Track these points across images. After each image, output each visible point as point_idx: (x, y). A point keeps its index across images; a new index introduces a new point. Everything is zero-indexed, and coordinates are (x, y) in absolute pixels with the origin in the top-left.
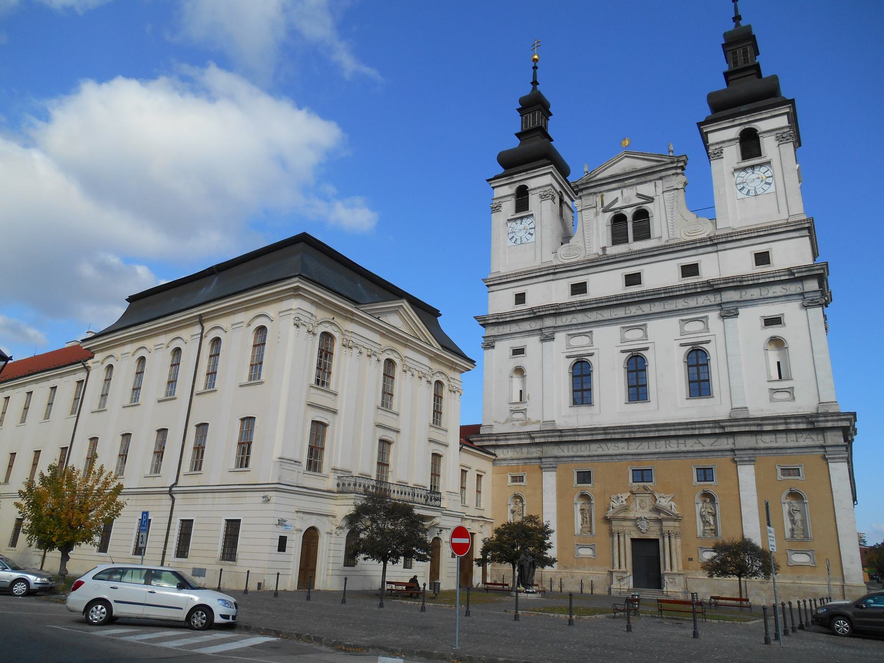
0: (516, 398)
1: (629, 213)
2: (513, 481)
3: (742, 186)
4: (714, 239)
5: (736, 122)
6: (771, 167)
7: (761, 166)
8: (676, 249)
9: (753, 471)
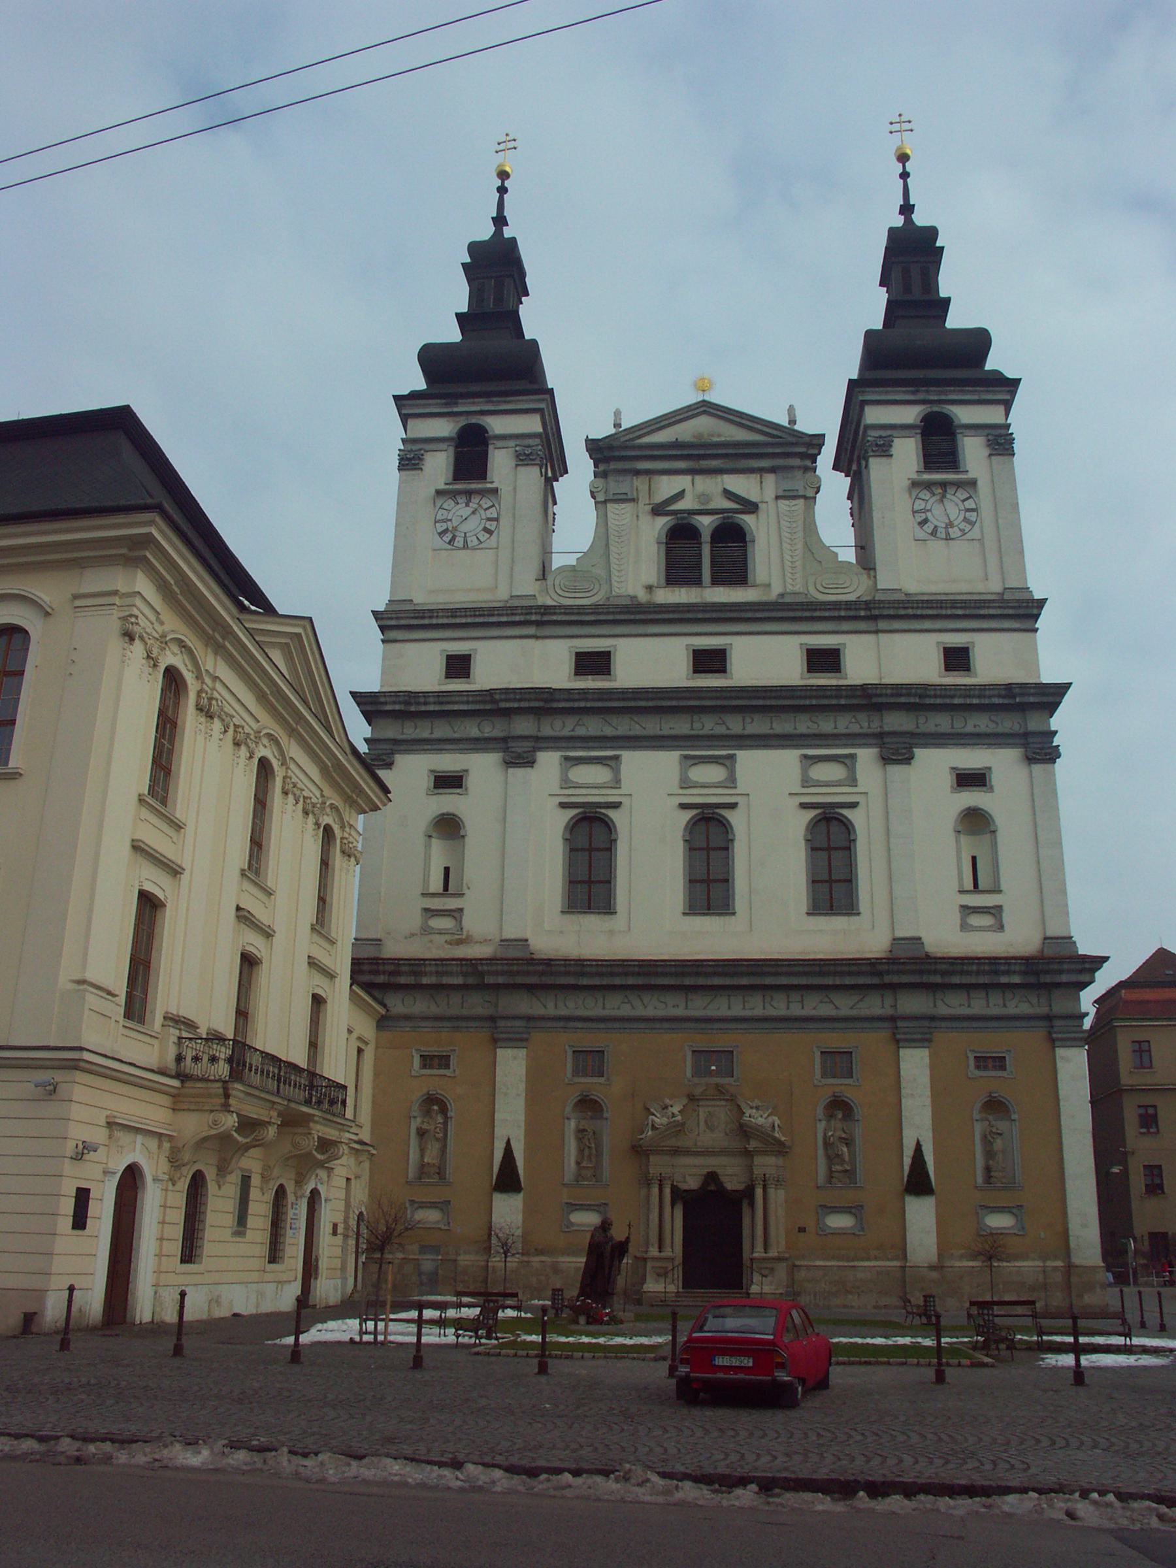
0: (436, 884)
1: (706, 523)
2: (424, 1066)
3: (923, 516)
4: (875, 608)
5: (921, 396)
6: (976, 491)
7: (959, 487)
8: (799, 614)
9: (927, 1060)
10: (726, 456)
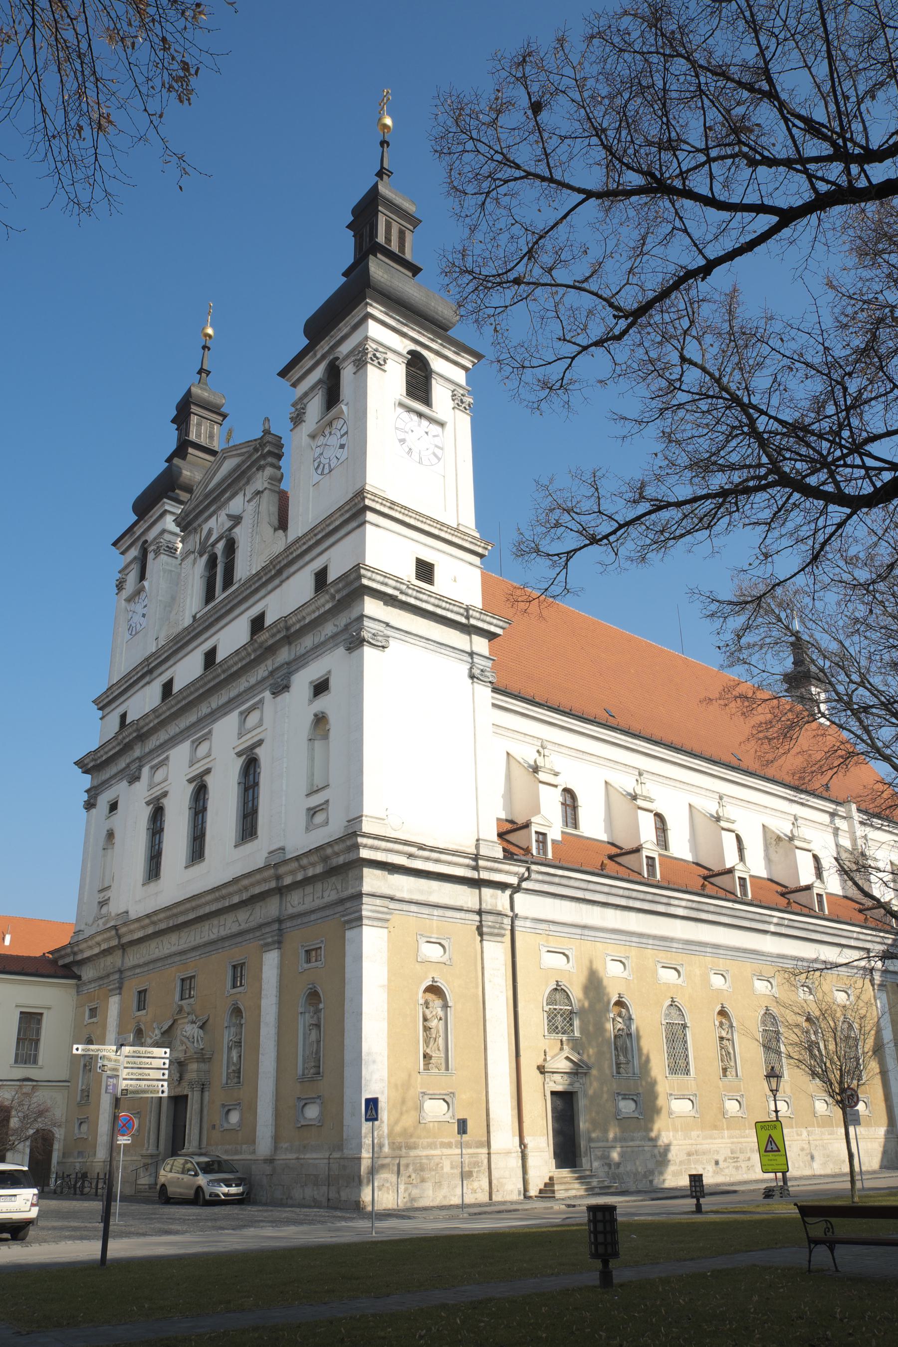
10: (229, 486)
